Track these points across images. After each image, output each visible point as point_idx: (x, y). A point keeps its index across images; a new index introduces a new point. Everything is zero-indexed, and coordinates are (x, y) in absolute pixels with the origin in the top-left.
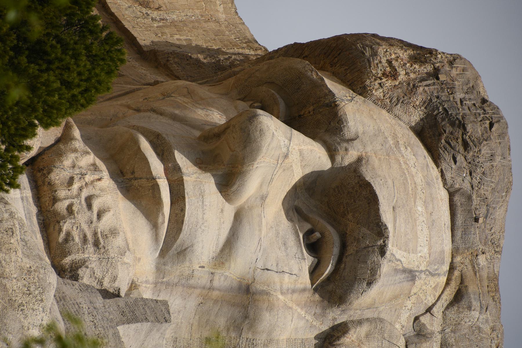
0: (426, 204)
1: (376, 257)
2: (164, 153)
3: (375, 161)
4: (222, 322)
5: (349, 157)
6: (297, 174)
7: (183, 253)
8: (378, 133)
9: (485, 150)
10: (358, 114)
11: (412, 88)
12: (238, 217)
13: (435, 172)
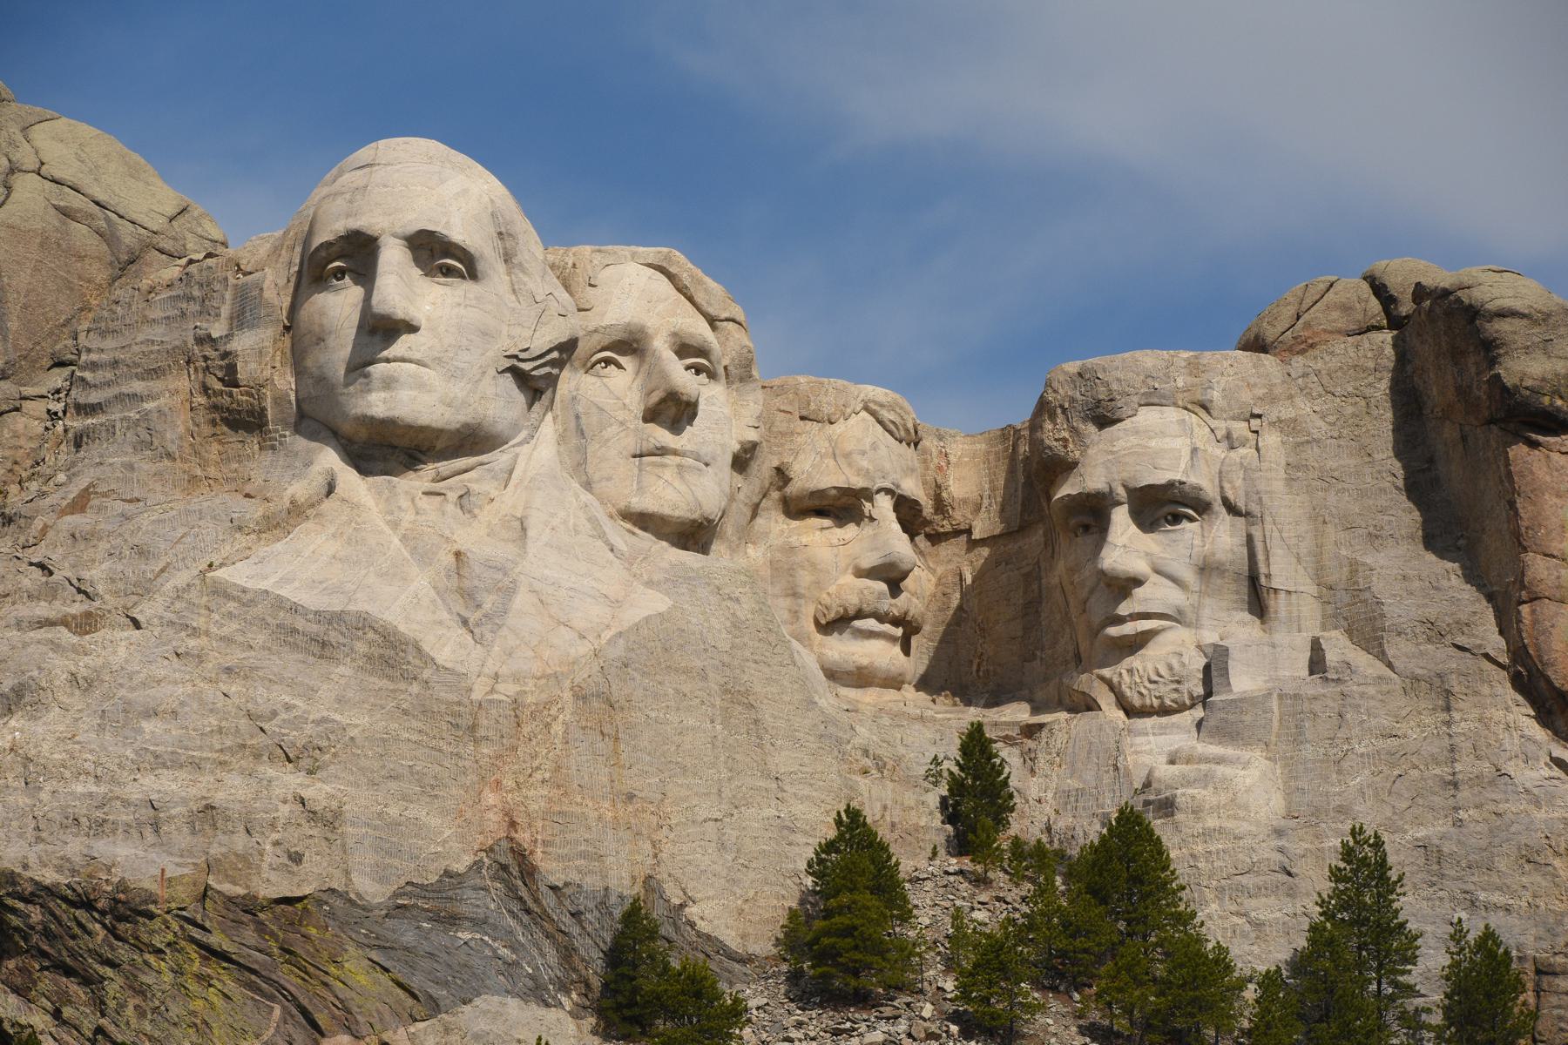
0: (1150, 438)
1: (1186, 488)
2: (1120, 620)
3: (1125, 475)
4: (1219, 581)
5: (1121, 492)
6: (1134, 529)
7: (1180, 612)
8: (1104, 463)
9: (1115, 386)
10: (1092, 477)
11: (1074, 430)
12: (1158, 572)
13: (1128, 421)
